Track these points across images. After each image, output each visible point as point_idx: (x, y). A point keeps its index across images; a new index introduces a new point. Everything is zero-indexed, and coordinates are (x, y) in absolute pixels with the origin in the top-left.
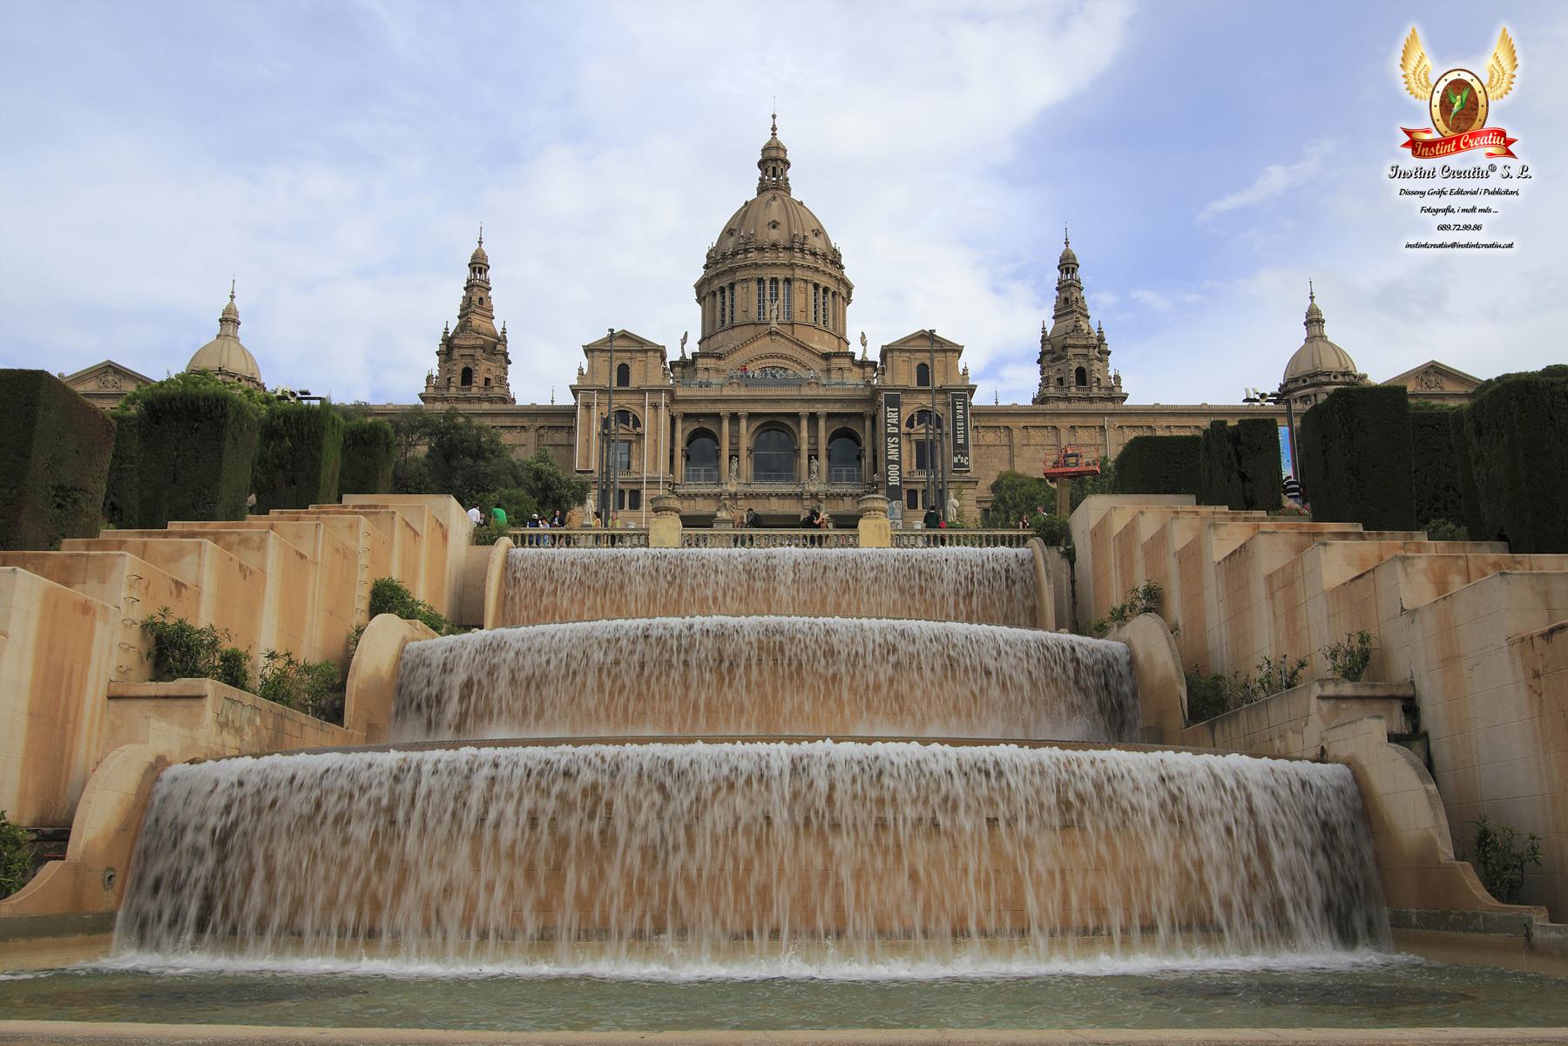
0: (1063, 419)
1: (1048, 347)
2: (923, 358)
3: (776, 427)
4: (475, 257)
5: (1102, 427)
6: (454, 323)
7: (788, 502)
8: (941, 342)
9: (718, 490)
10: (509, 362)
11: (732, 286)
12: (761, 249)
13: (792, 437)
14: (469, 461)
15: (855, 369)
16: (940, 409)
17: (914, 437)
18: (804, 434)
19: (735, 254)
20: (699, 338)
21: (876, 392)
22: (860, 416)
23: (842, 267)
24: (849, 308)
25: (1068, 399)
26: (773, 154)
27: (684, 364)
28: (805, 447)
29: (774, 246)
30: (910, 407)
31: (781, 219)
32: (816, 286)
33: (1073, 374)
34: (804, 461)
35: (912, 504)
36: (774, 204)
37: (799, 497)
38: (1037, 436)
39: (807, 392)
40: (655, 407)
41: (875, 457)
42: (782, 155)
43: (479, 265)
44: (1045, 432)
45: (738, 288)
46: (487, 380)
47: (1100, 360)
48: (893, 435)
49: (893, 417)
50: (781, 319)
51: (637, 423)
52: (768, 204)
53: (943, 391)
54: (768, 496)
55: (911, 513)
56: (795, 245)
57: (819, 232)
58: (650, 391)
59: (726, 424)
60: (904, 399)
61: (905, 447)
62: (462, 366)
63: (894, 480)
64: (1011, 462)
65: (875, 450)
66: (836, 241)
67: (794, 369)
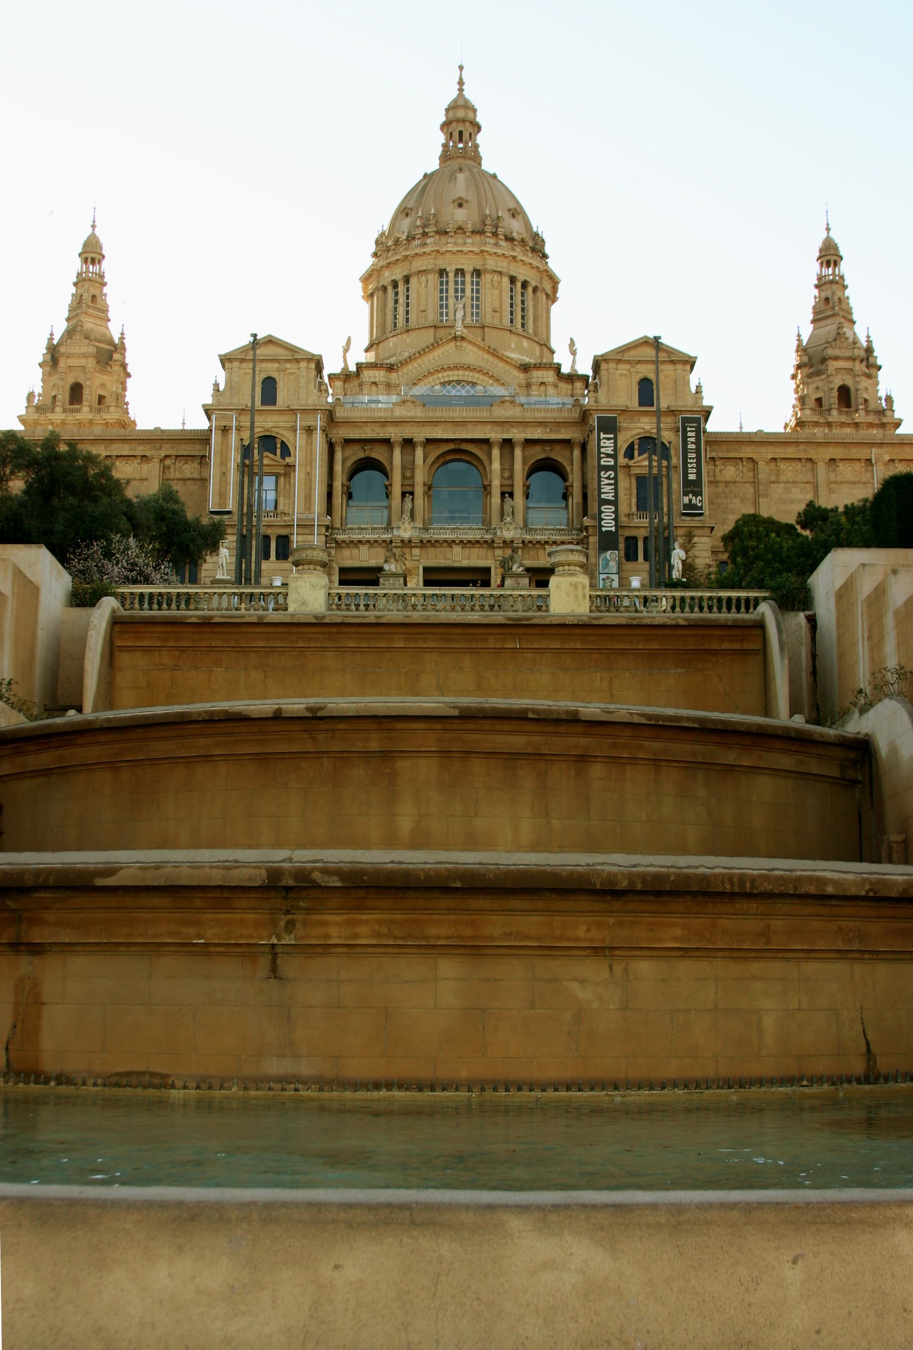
0: (821, 450)
1: (805, 359)
2: (646, 370)
3: (459, 454)
4: (86, 245)
5: (870, 460)
7: (475, 551)
8: (670, 351)
9: (386, 536)
10: (129, 375)
11: (407, 279)
13: (480, 466)
14: (71, 501)
15: (562, 385)
16: (667, 436)
17: (635, 471)
18: (496, 466)
19: (410, 238)
20: (366, 343)
21: (585, 415)
22: (567, 442)
23: (545, 256)
24: (555, 309)
25: (829, 425)
26: (461, 113)
27: (346, 377)
28: (496, 483)
29: (460, 229)
31: (471, 196)
32: (513, 280)
33: (835, 394)
34: (496, 499)
35: (630, 555)
36: (461, 177)
37: (490, 544)
38: (788, 471)
39: (501, 413)
40: (309, 430)
41: (585, 496)
42: (470, 115)
43: (92, 253)
44: (798, 466)
45: (413, 281)
46: (101, 399)
47: (869, 376)
48: (607, 468)
49: (607, 446)
50: (468, 320)
51: (286, 451)
52: (452, 177)
53: (672, 412)
54: (451, 543)
55: (629, 566)
57: (517, 212)
58: (304, 411)
59: (397, 453)
60: (623, 422)
61: (623, 483)
62: (71, 380)
63: (608, 525)
64: (756, 503)
65: (584, 487)
66: (538, 223)
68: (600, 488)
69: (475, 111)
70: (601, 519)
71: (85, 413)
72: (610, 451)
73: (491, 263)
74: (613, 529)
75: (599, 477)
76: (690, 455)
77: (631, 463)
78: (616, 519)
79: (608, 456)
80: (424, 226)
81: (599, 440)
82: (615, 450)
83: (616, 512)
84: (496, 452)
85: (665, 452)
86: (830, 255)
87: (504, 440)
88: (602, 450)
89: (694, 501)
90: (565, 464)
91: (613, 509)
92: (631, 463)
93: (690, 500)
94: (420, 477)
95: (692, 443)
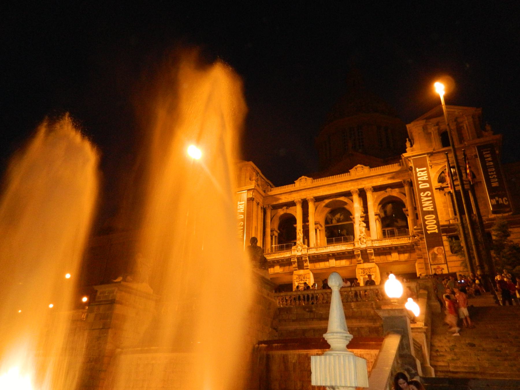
22: (399, 185)
68: (421, 204)
70: (425, 225)
72: (425, 179)
74: (437, 231)
75: (420, 197)
76: (489, 170)
77: (444, 185)
78: (438, 224)
79: (424, 182)
81: (416, 173)
82: (429, 177)
83: (437, 218)
84: (356, 197)
87: (359, 189)
88: (419, 179)
89: (501, 202)
90: (402, 199)
91: (434, 216)
92: (444, 185)
93: (497, 202)
95: (490, 161)
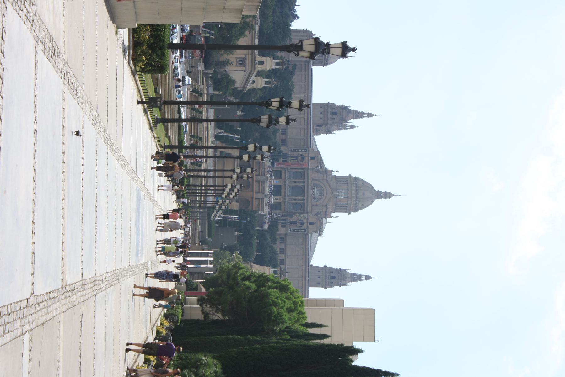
6: (352, 109)
12: (357, 190)
18: (300, 198)
22: (304, 210)
23: (354, 212)
29: (357, 194)
30: (305, 221)
34: (294, 197)
37: (285, 196)
43: (370, 115)
53: (308, 227)
56: (358, 199)
67: (324, 197)
69: (389, 198)
71: (330, 116)
73: (349, 200)
80: (358, 187)
85: (300, 227)
86: (368, 278)
94: (298, 184)
